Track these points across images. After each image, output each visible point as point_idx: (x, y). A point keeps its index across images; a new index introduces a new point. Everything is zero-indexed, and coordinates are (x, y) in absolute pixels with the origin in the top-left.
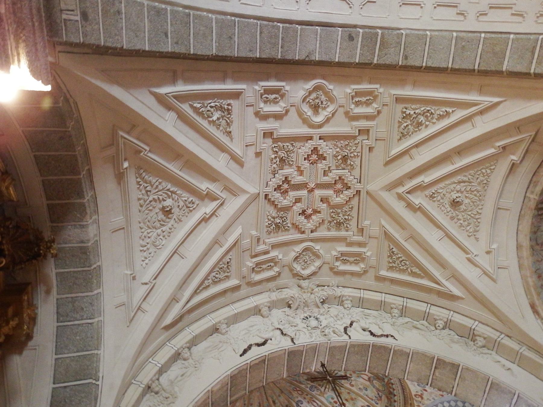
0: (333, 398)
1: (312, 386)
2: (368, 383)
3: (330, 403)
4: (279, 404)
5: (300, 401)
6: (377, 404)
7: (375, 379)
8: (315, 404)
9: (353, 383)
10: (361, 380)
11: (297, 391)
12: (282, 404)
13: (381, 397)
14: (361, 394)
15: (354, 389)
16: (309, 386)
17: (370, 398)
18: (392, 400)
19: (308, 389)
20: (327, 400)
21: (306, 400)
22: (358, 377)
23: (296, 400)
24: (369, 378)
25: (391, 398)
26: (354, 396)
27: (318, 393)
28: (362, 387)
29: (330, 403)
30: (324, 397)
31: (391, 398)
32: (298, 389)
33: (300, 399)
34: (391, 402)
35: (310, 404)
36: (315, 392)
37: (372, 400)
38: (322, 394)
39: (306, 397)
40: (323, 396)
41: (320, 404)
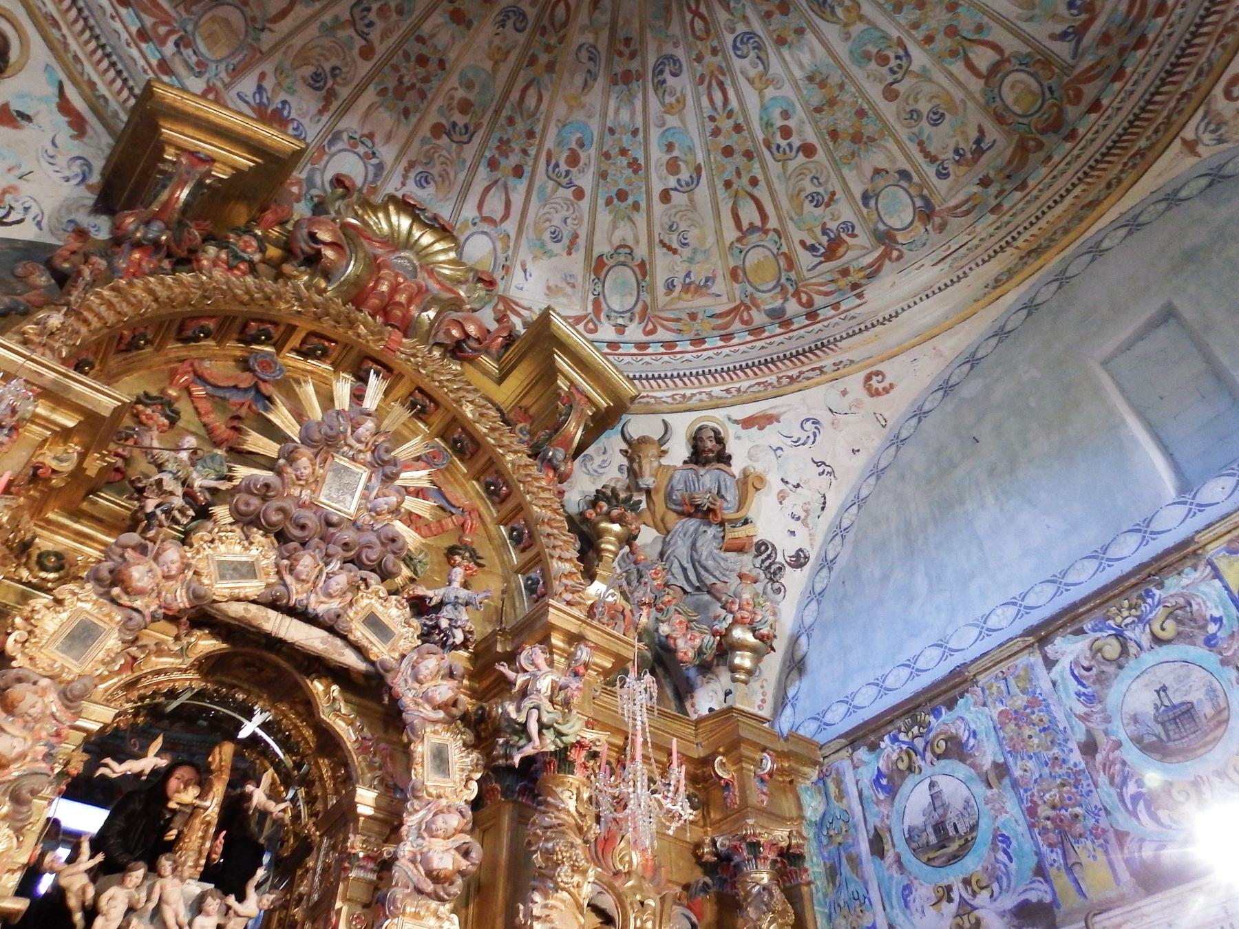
0: (786, 115)
1: (752, 34)
2: (976, 85)
3: (768, 124)
4: (605, 18)
5: (676, 61)
6: (942, 175)
7: (1025, 63)
8: (718, 96)
9: (901, 88)
10: (958, 68)
11: (696, 13)
12: (621, 22)
13: (979, 152)
14: (903, 133)
15: (888, 110)
16: (741, 28)
17: (927, 154)
18: (1034, 158)
19: (729, 38)
20: (764, 108)
21: (699, 69)
22: (954, 53)
23: (668, 49)
24: (995, 68)
25: (1040, 145)
26: (870, 128)
27: (753, 73)
28: (924, 107)
29: (768, 124)
30: (761, 96)
31: (1040, 145)
32: (703, 9)
33: (680, 53)
34: (1023, 162)
35: (703, 89)
36: (745, 62)
37: (933, 159)
38: (764, 80)
39: (708, 58)
40: (761, 91)
41: (734, 103)
